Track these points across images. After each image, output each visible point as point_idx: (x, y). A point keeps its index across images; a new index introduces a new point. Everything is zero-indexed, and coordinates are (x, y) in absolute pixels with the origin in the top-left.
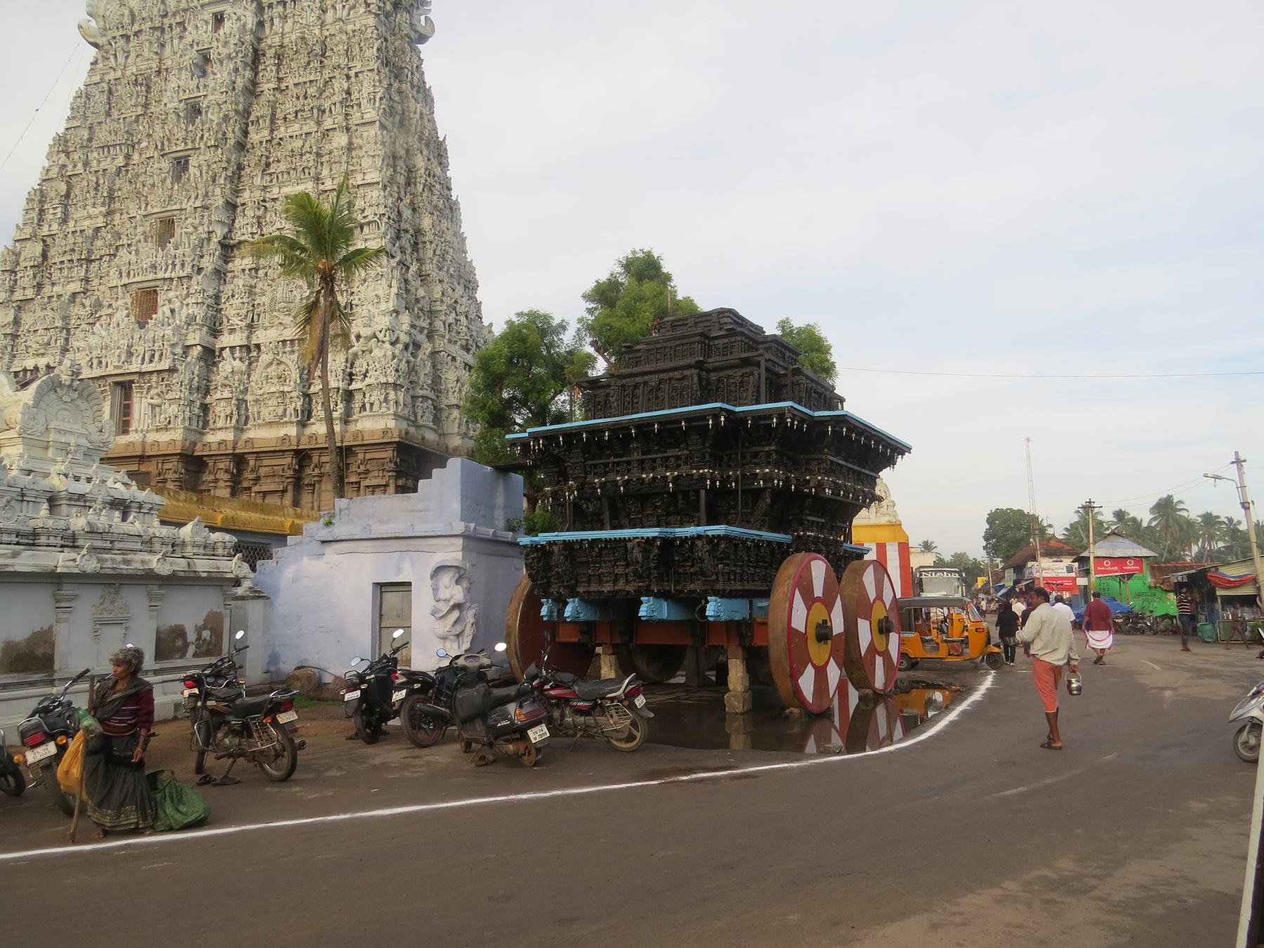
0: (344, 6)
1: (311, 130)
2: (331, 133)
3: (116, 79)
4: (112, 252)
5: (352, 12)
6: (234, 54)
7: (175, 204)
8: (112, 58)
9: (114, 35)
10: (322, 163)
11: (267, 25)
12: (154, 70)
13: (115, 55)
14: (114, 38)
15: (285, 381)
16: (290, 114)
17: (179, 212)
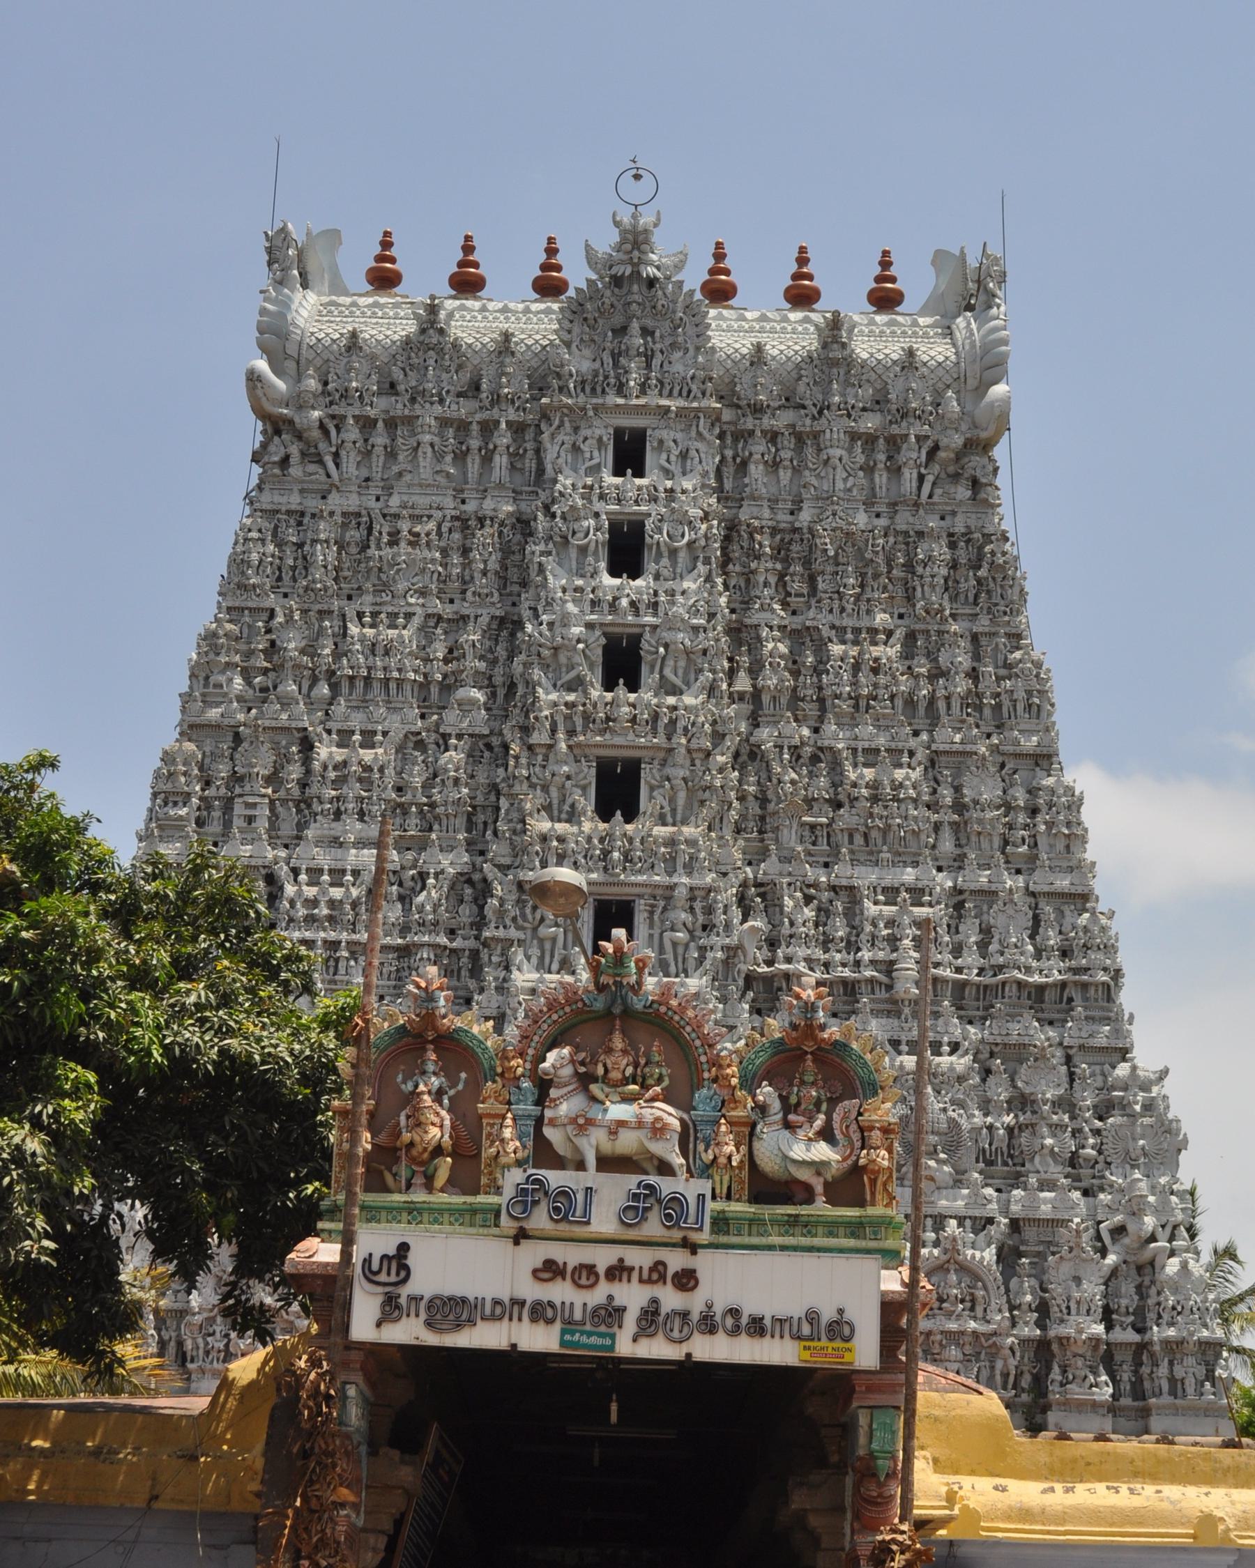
0: (921, 478)
1: (900, 745)
2: (943, 759)
3: (344, 514)
4: (443, 940)
5: (938, 491)
6: (703, 542)
7: (640, 872)
8: (329, 460)
9: (336, 410)
10: (937, 827)
11: (729, 471)
12: (450, 513)
13: (336, 455)
14: (333, 417)
15: (972, 1309)
16: (837, 697)
17: (649, 891)
